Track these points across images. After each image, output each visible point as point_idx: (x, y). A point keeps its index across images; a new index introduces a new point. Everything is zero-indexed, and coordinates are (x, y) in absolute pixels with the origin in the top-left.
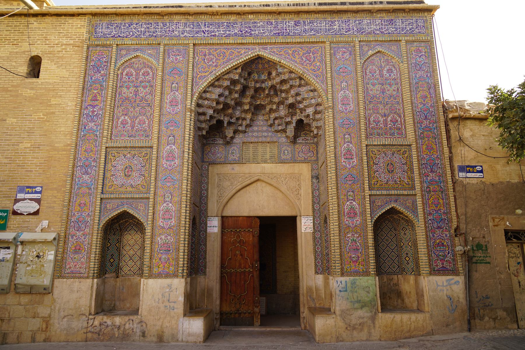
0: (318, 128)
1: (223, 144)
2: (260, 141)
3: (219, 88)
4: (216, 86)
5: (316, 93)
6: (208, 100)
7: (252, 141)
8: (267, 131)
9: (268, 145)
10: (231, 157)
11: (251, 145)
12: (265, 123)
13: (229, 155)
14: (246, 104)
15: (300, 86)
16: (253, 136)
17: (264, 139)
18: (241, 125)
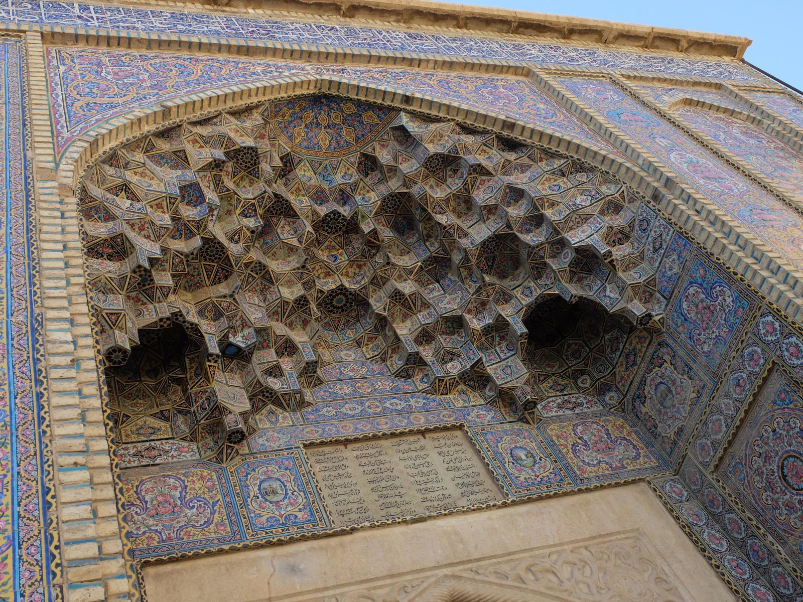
0: (646, 291)
1: (200, 463)
2: (385, 428)
3: (175, 167)
4: (160, 159)
5: (582, 177)
6: (133, 197)
7: (350, 433)
8: (395, 393)
9: (427, 442)
10: (264, 514)
11: (349, 453)
12: (377, 367)
13: (253, 506)
14: (290, 284)
15: (506, 168)
16: (343, 417)
17: (402, 425)
18: (275, 371)
